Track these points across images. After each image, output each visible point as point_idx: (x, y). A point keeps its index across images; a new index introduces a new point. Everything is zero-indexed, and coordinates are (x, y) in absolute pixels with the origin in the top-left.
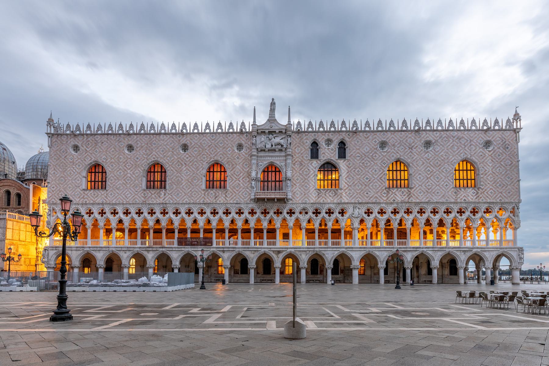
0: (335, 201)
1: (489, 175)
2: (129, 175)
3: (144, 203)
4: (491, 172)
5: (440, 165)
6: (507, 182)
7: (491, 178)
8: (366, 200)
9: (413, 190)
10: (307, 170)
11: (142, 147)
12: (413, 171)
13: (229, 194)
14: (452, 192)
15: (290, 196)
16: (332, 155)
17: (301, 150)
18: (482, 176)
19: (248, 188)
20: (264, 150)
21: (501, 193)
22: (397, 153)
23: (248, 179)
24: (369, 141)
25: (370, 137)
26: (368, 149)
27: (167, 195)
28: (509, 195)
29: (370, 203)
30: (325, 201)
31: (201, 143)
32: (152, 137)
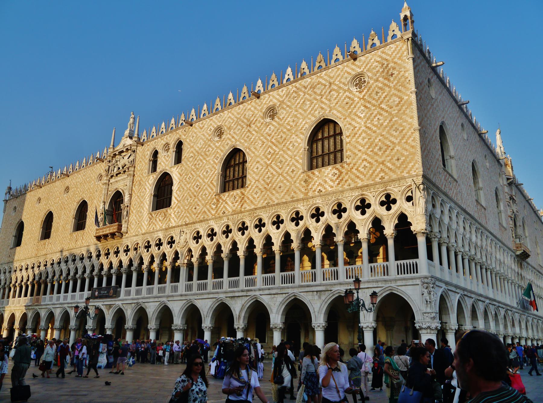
0: (164, 227)
1: (359, 137)
3: (36, 256)
4: (364, 128)
5: (285, 139)
6: (393, 139)
7: (363, 139)
8: (194, 218)
9: (248, 189)
14: (300, 181)
18: (348, 140)
21: (383, 163)
22: (233, 137)
25: (206, 126)
28: (398, 164)
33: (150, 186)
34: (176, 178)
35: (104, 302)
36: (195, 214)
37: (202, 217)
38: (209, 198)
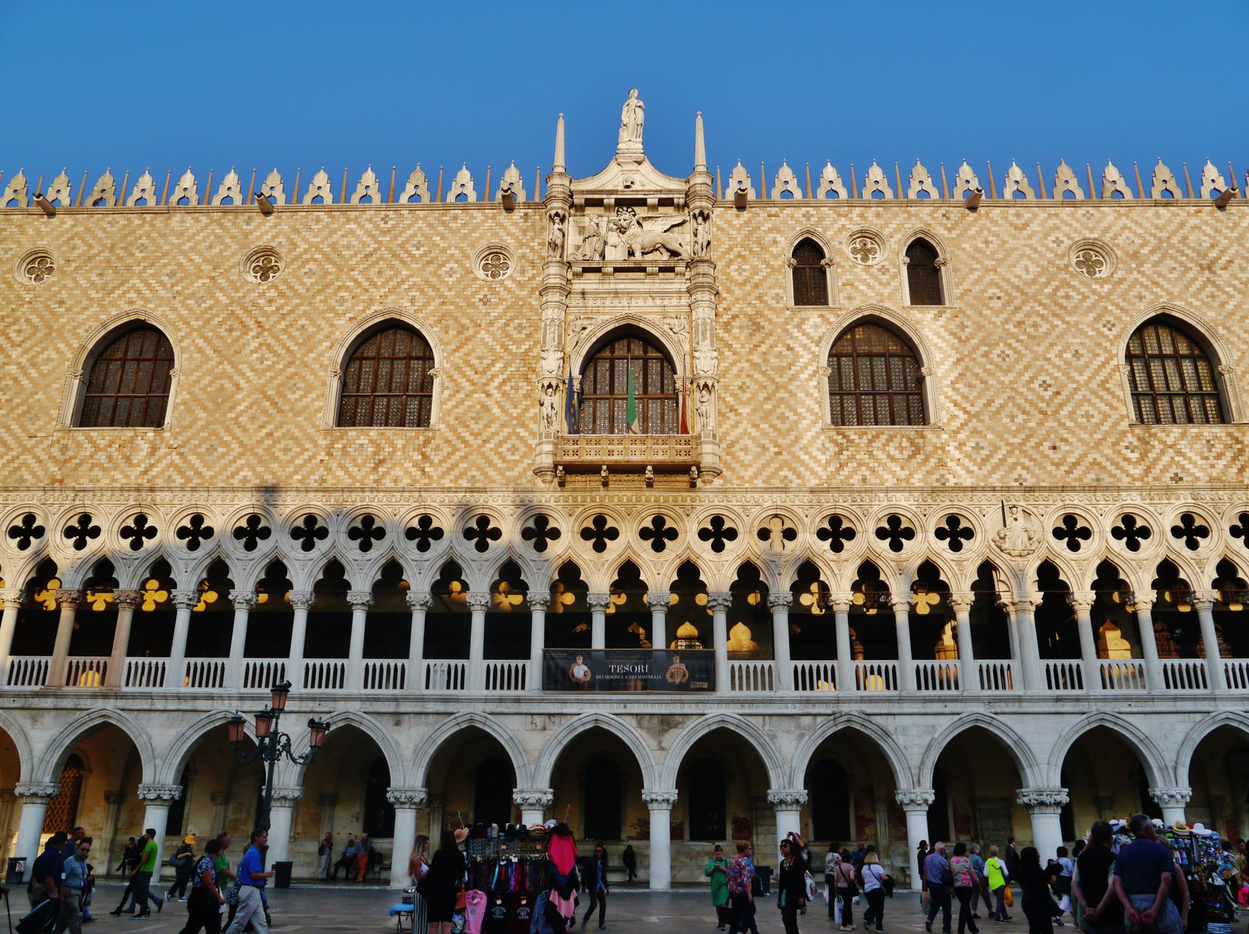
0: (917, 481)
2: (13, 369)
8: (1058, 475)
10: (780, 348)
11: (90, 259)
12: (1236, 355)
13: (437, 449)
15: (707, 461)
16: (886, 292)
17: (755, 271)
19: (523, 425)
20: (598, 270)
22: (1157, 284)
23: (524, 387)
24: (1033, 242)
25: (1035, 226)
26: (1034, 269)
27: (163, 450)
29: (1073, 489)
30: (873, 480)
31: (334, 246)
33: (818, 343)
34: (944, 345)
35: (625, 702)
36: (1057, 465)
37: (1092, 476)
38: (1106, 427)
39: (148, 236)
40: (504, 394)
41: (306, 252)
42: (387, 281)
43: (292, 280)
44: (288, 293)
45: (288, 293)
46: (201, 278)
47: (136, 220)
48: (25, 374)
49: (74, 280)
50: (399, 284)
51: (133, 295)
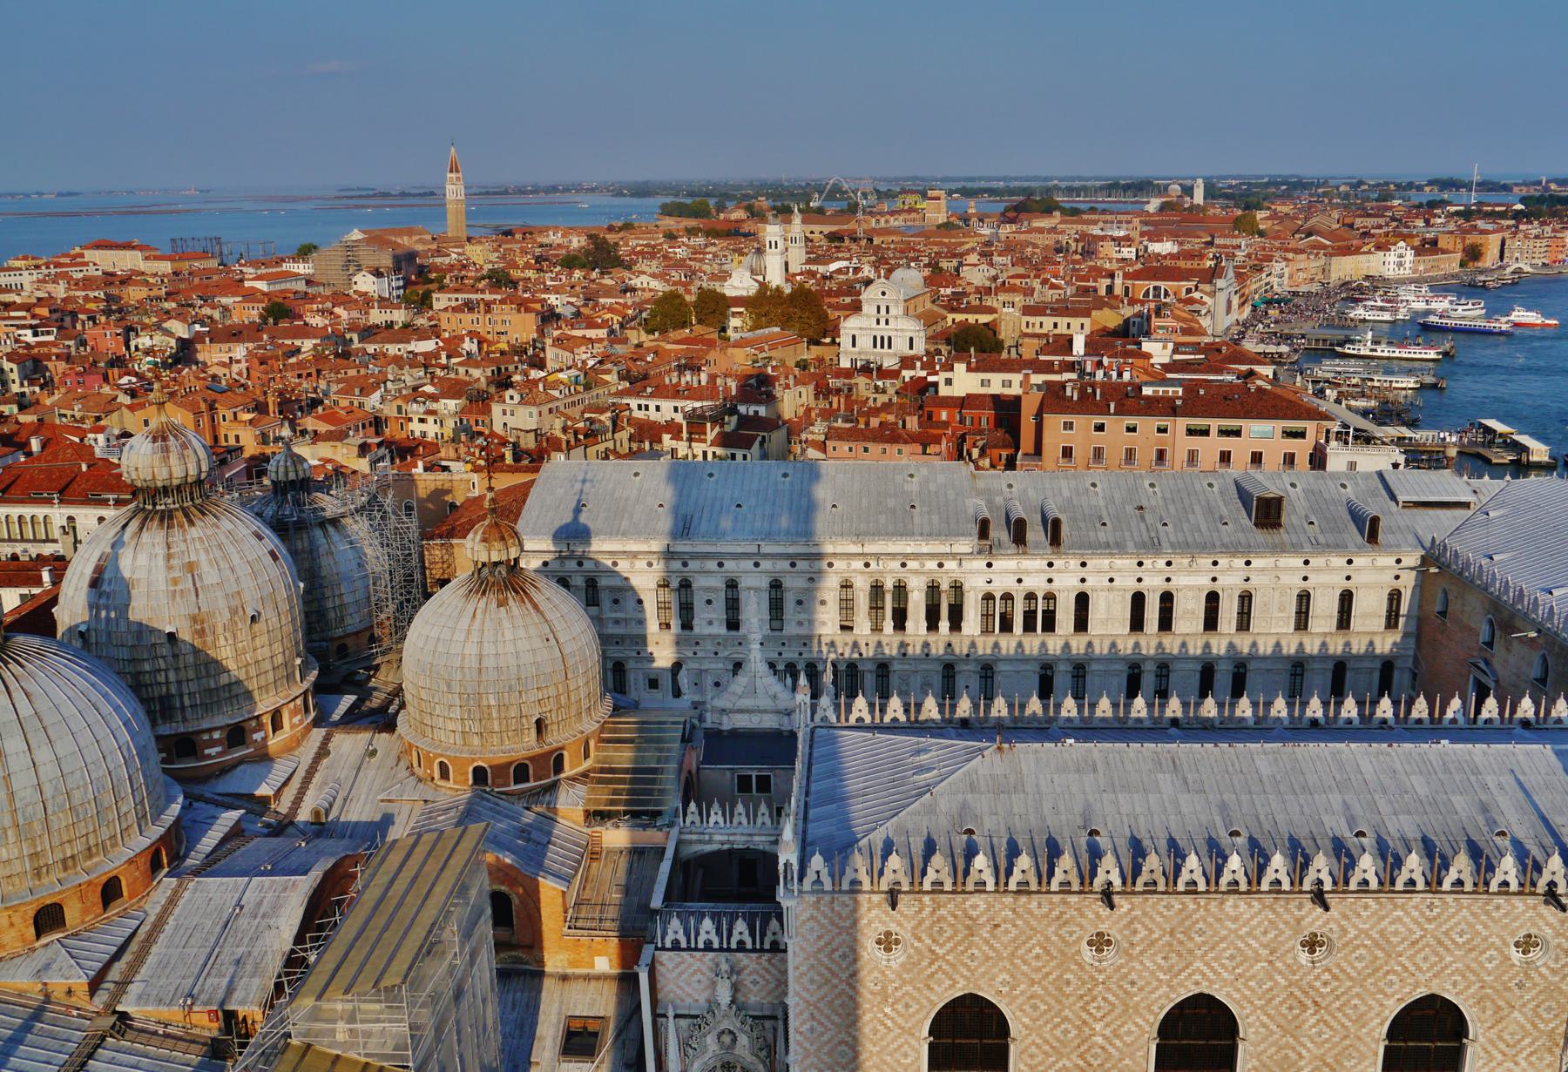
2: (1099, 1040)
11: (1153, 943)
31: (1382, 933)
32: (1192, 906)
39: (1205, 921)
40: (1531, 1063)
41: (1356, 938)
42: (1432, 966)
43: (1344, 964)
44: (1341, 976)
45: (1341, 976)
46: (1258, 961)
47: (1187, 899)
48: (1113, 1045)
49: (1141, 962)
50: (1443, 969)
51: (1197, 977)
